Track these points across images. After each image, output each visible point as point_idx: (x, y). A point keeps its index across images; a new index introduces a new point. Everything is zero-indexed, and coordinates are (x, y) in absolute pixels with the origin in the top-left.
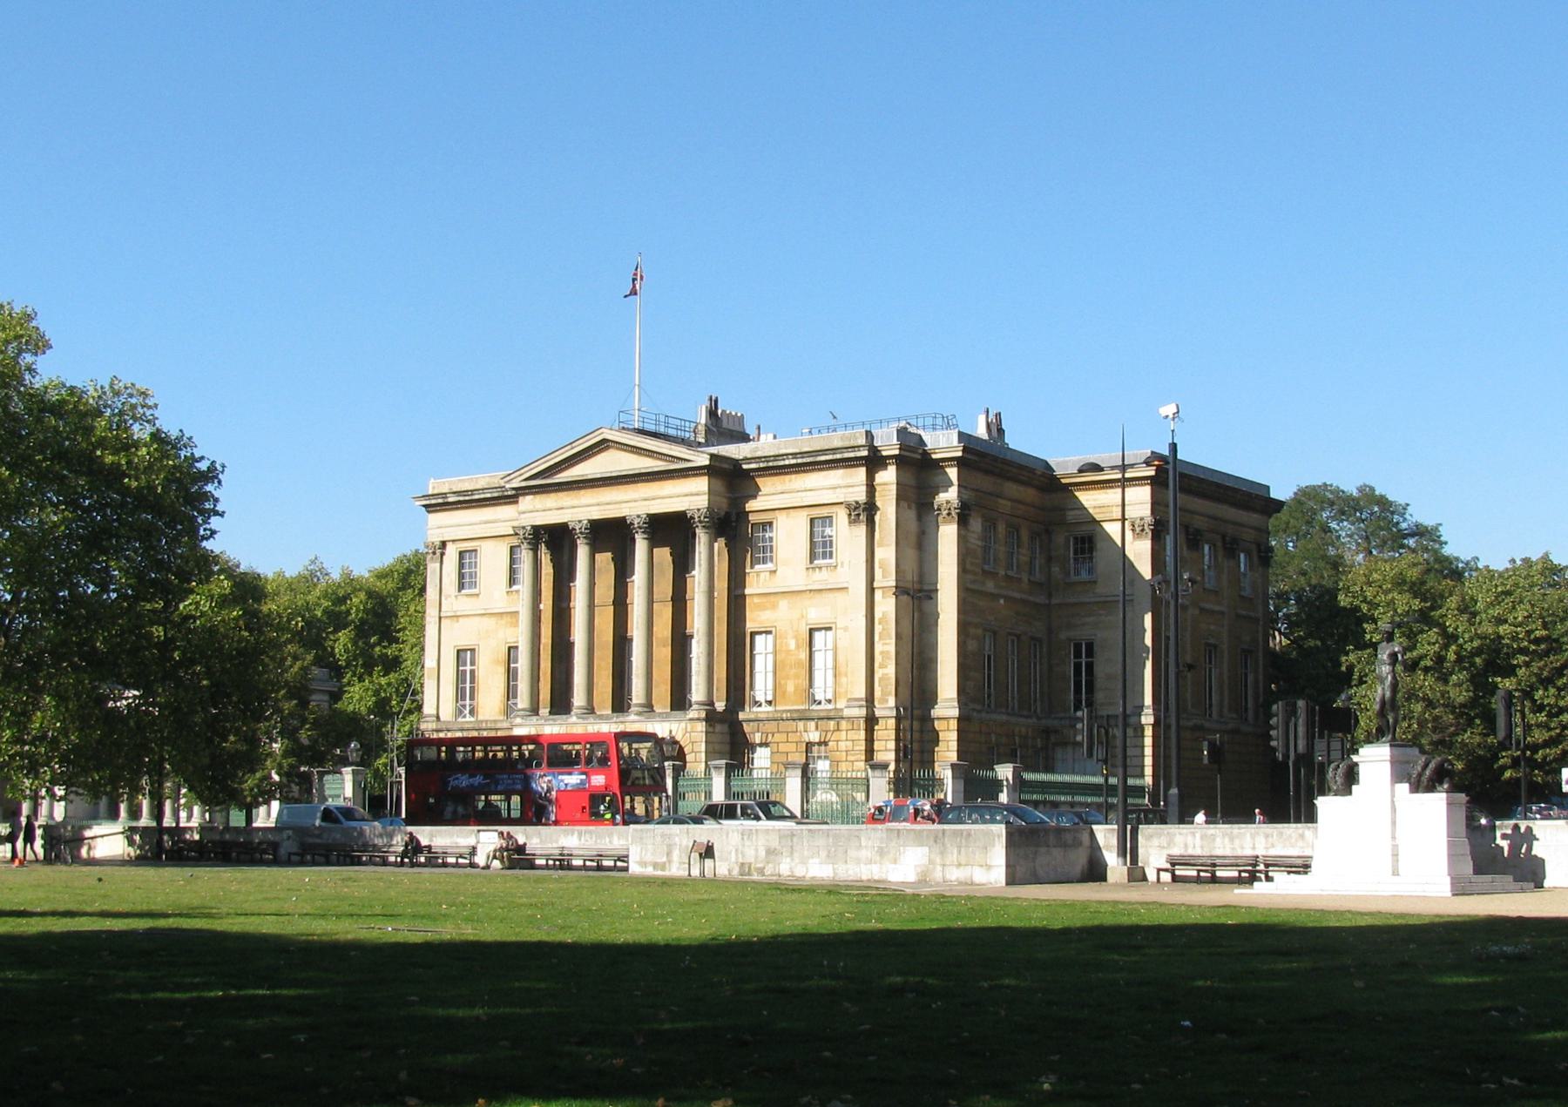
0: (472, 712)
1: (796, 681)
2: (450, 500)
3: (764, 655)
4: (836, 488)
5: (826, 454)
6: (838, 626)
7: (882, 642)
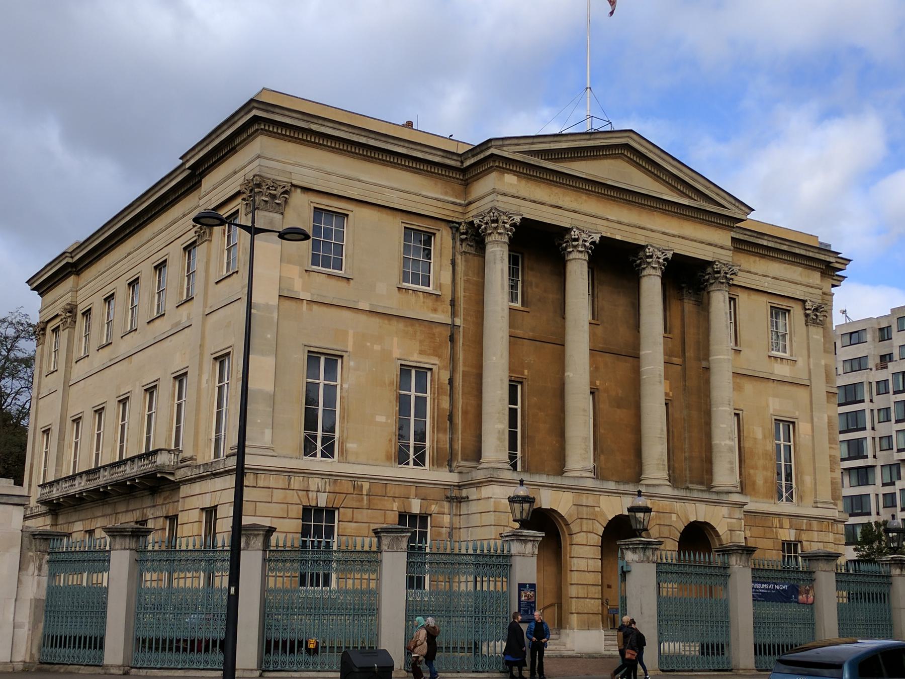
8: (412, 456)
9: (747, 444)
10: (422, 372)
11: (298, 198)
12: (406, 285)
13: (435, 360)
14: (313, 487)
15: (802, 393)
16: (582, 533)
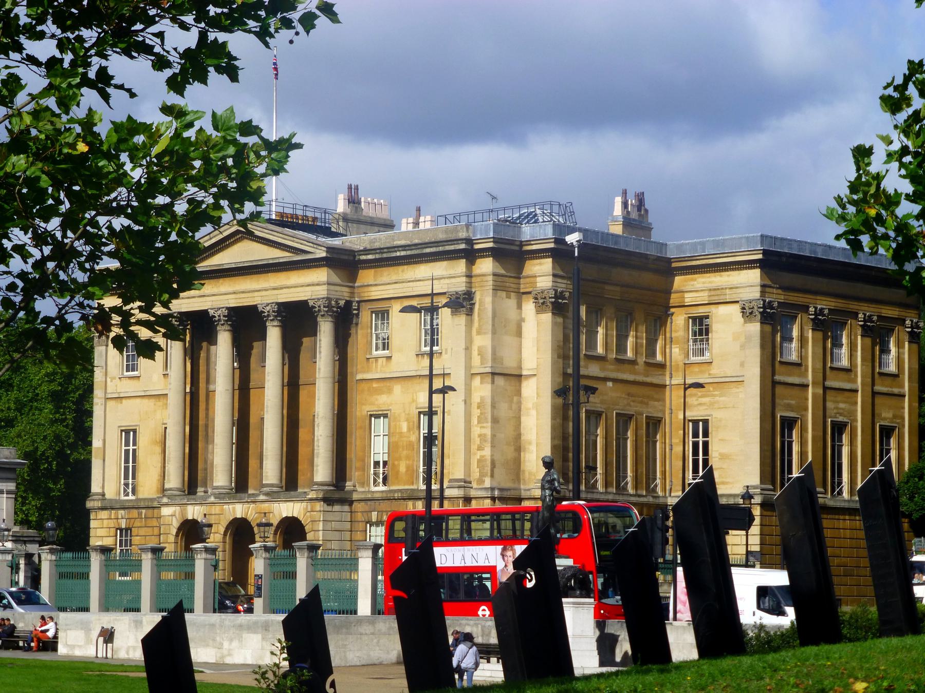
0: (134, 492)
1: (407, 462)
3: (382, 436)
5: (431, 247)
7: (480, 425)
14: (120, 517)
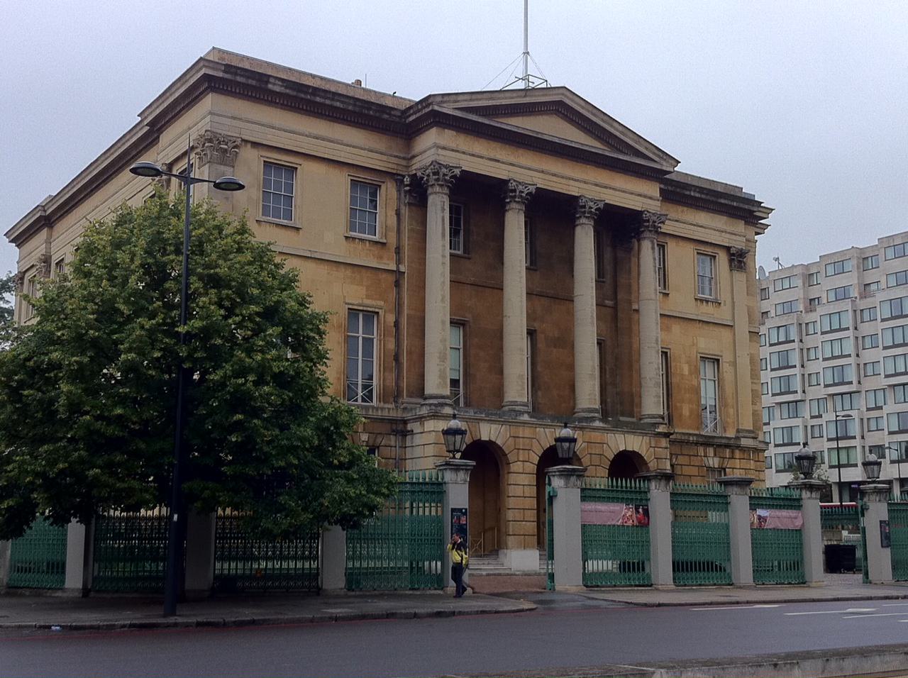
2: (270, 86)
4: (722, 232)
6: (724, 360)
8: (360, 394)
9: (675, 380)
10: (370, 316)
11: (248, 154)
12: (353, 234)
13: (382, 303)
15: (726, 333)
16: (519, 463)
